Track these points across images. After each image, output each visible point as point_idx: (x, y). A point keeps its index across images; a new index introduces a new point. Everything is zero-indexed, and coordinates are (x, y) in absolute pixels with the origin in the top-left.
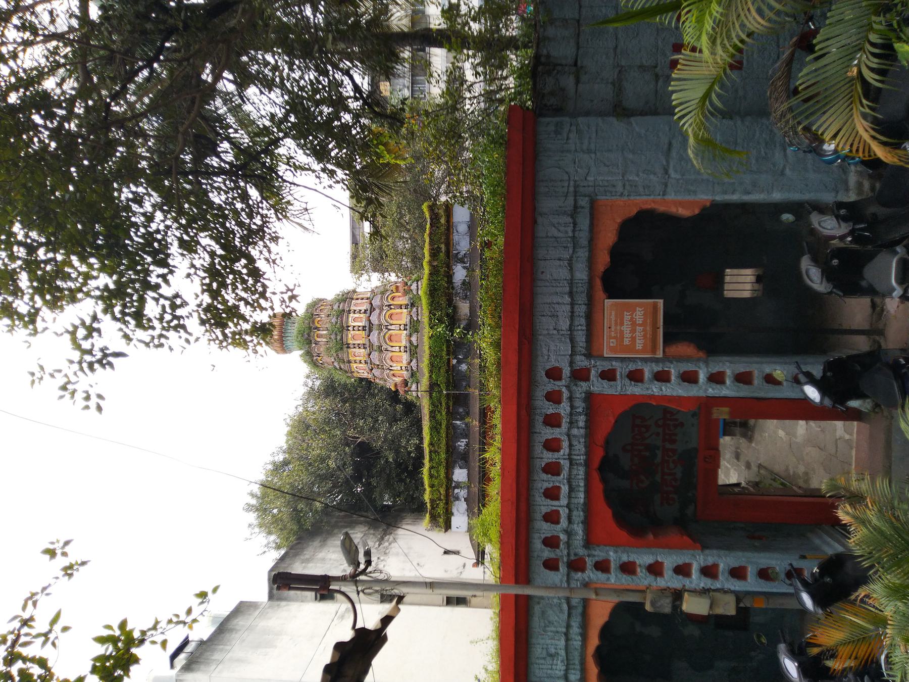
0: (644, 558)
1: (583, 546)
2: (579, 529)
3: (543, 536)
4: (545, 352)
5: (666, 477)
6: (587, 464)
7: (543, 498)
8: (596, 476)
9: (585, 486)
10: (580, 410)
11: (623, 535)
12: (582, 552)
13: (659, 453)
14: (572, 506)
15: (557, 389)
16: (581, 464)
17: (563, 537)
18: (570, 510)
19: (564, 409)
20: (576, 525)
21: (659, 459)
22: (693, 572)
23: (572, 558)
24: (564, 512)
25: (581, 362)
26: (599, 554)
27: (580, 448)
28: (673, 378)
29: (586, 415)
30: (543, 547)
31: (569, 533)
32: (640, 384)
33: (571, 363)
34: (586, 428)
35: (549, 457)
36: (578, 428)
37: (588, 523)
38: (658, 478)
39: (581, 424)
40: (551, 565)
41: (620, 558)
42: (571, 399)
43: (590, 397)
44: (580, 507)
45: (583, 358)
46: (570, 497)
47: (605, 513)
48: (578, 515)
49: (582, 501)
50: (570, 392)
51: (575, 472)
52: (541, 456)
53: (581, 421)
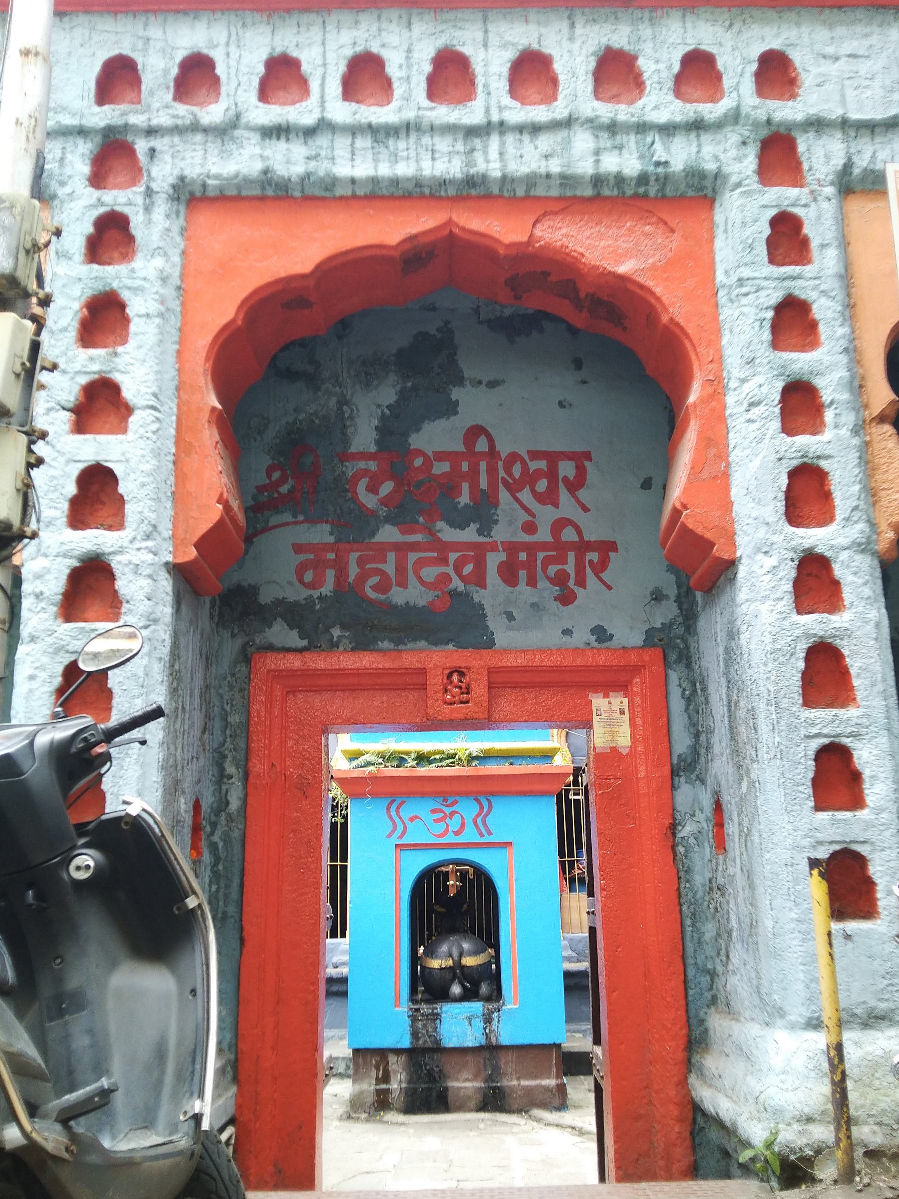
0: (142, 365)
1: (182, 179)
2: (244, 161)
3: (217, 55)
4: (847, 48)
5: (391, 557)
6: (473, 191)
7: (349, 52)
8: (421, 223)
9: (395, 182)
10: (660, 153)
11: (223, 310)
12: (162, 175)
13: (470, 535)
14: (322, 141)
15: (727, 82)
16: (470, 164)
17: (213, 113)
18: (309, 133)
19: (659, 103)
20: (257, 151)
21: (448, 533)
22: (90, 533)
23: (141, 146)
24: (302, 114)
25: (821, 157)
26: (156, 231)
27: (524, 159)
28: (802, 440)
29: (643, 179)
30: (180, 56)
31: (224, 132)
32: (767, 335)
33: (817, 125)
34: (598, 181)
35: (492, 64)
36: (597, 152)
37: (271, 195)
38: (388, 534)
39: (611, 164)
40: (117, 78)
41: (135, 290)
42: (697, 126)
43: (697, 194)
44: (322, 168)
45: (838, 161)
46: (354, 131)
47: (301, 249)
48: (290, 161)
49: (343, 170)
50: (719, 126)
51: (443, 144)
52: (493, 39)
53: (626, 162)
